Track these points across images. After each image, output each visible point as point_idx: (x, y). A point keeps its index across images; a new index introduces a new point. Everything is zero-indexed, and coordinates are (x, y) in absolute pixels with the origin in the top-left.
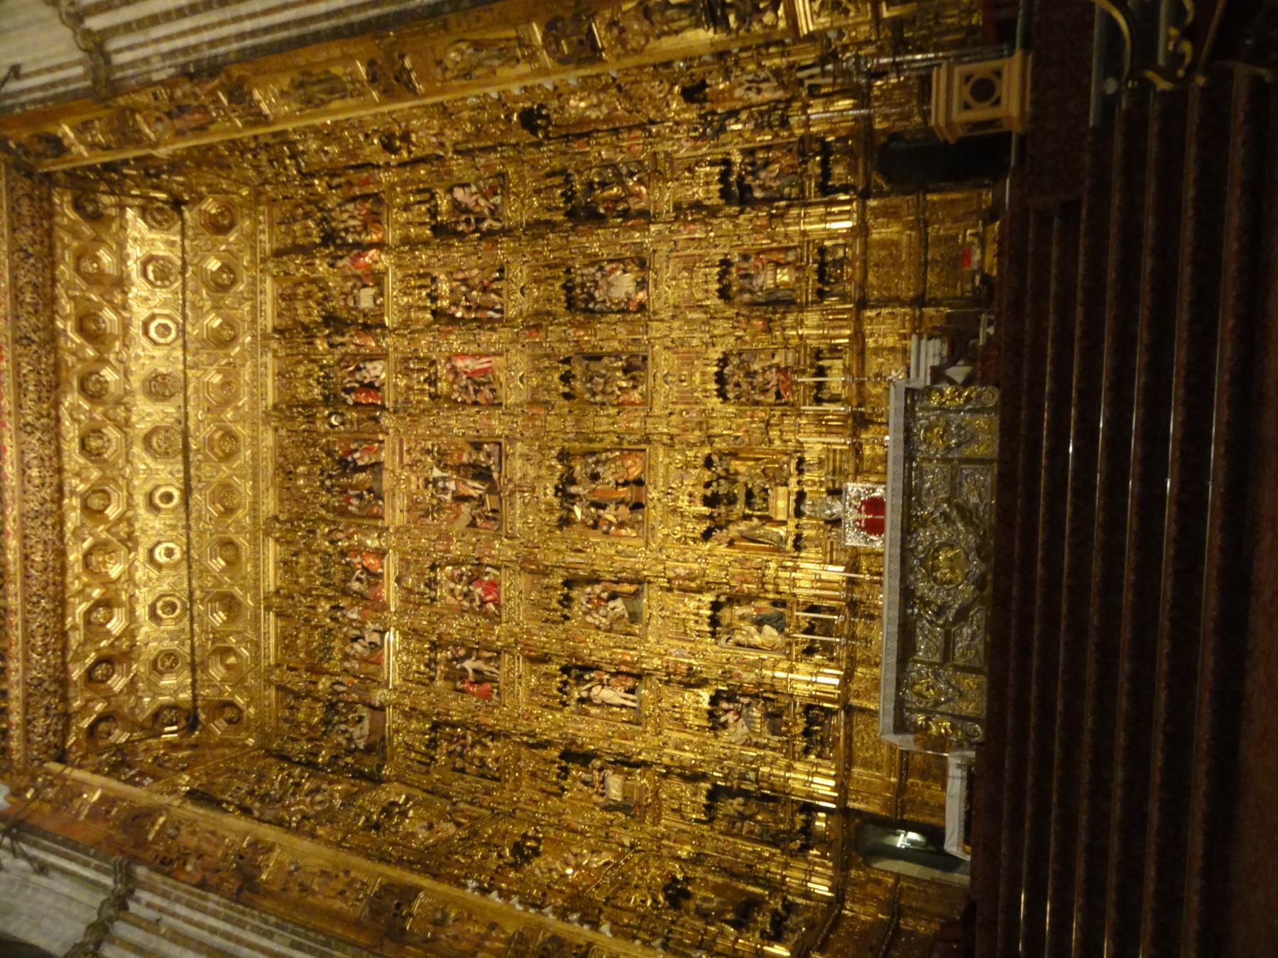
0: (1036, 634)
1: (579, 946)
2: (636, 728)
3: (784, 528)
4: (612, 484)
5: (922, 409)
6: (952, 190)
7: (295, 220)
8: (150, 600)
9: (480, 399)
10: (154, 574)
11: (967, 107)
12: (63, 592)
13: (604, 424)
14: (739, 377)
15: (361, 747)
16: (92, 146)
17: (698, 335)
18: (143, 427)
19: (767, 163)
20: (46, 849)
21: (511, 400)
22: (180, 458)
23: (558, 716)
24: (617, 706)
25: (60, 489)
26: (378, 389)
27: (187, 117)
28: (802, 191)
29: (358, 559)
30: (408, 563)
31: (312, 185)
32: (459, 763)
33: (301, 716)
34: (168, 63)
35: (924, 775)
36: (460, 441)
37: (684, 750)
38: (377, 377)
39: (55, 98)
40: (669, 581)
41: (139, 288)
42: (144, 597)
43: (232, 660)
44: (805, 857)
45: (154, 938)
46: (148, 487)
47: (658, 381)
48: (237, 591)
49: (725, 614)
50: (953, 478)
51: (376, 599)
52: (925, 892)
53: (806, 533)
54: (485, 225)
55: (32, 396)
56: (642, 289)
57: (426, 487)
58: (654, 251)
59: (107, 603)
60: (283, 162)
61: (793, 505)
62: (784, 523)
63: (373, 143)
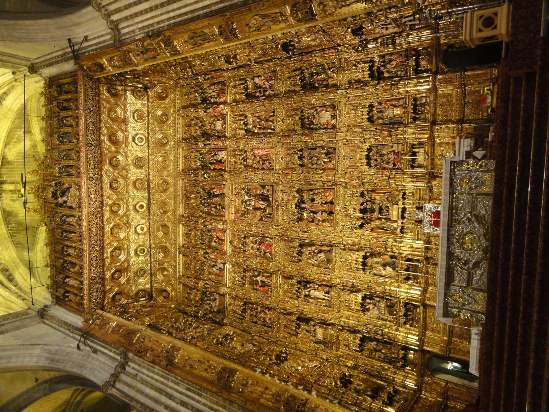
0: (510, 275)
1: (302, 400)
2: (329, 309)
3: (396, 224)
4: (320, 203)
5: (458, 170)
6: (478, 70)
7: (191, 94)
8: (135, 247)
9: (265, 167)
10: (136, 237)
11: (480, 30)
12: (103, 243)
13: (316, 177)
14: (377, 156)
15: (215, 310)
16: (114, 67)
18: (133, 178)
19: (390, 61)
20: (96, 343)
21: (278, 167)
22: (146, 191)
23: (296, 302)
25: (102, 203)
26: (223, 163)
27: (149, 53)
28: (406, 73)
29: (215, 233)
30: (235, 235)
31: (197, 79)
32: (255, 320)
33: (192, 297)
34: (142, 32)
35: (460, 337)
36: (256, 185)
37: (350, 320)
39: (100, 48)
40: (344, 246)
41: (131, 122)
42: (133, 246)
43: (166, 273)
44: (404, 370)
45: (135, 381)
46: (135, 203)
47: (340, 159)
48: (168, 245)
49: (369, 261)
50: (473, 202)
51: (222, 250)
52: (460, 390)
53: (406, 226)
54: (267, 93)
55: (92, 166)
56: (334, 119)
57: (242, 204)
58: (339, 102)
59: (119, 248)
61: (400, 214)
62: (396, 221)
63: (221, 61)
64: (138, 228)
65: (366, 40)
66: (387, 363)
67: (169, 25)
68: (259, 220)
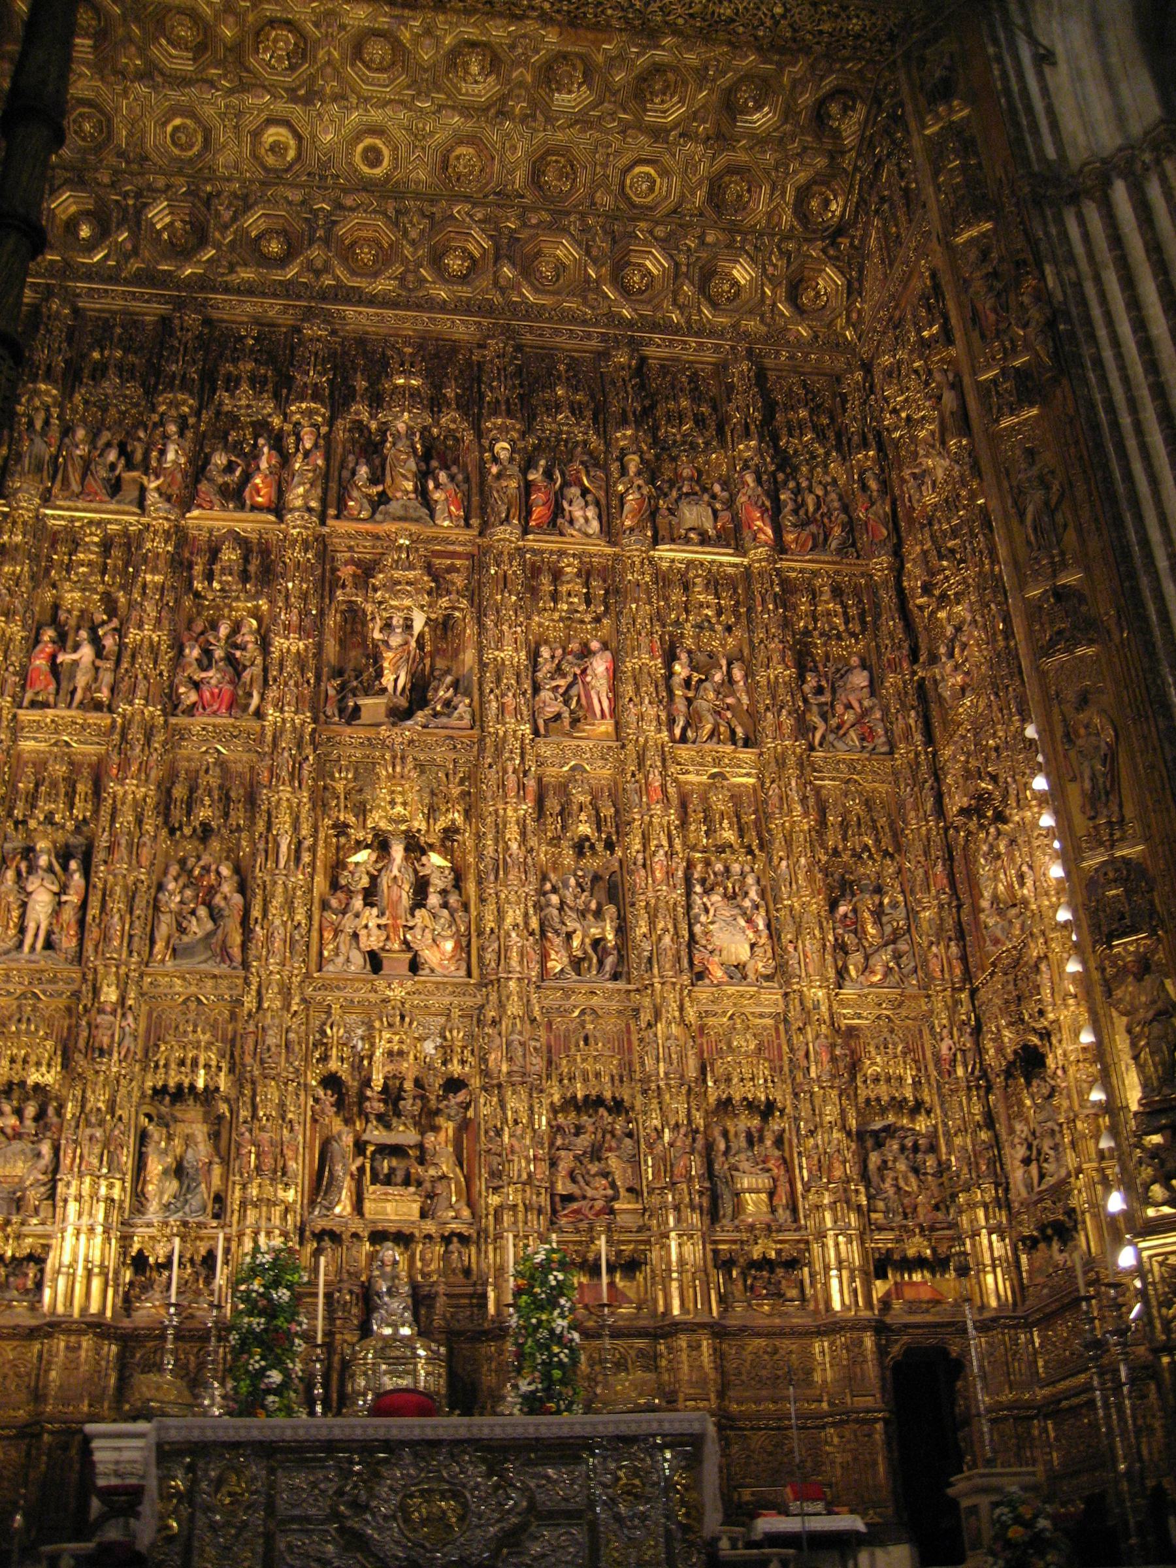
7: (812, 412)
9: (545, 695)
10: (251, 122)
19: (916, 1170)
24: (23, 916)
28: (880, 1229)
31: (865, 445)
38: (571, 522)
39: (1012, 110)
43: (85, 232)
60: (902, 408)
64: (283, 131)
65: (989, 1089)
67: (1092, 406)
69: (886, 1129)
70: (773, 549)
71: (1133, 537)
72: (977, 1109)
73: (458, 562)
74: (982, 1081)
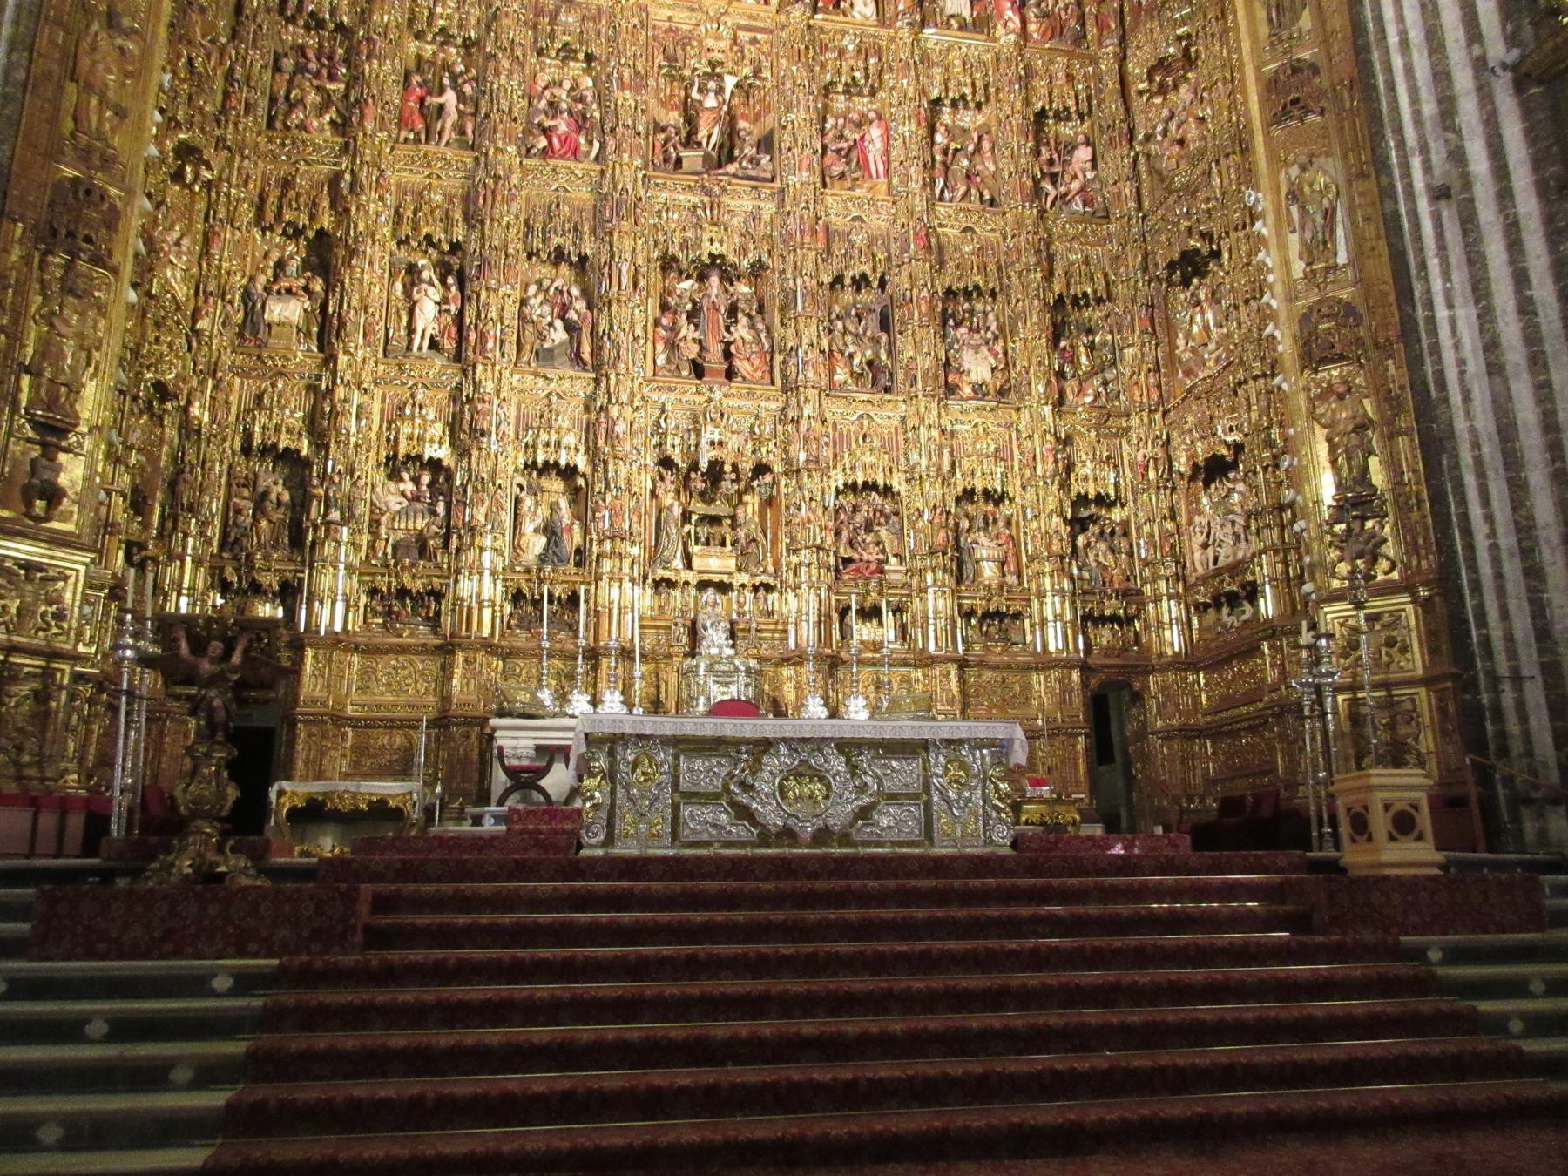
1: (110, 253)
3: (680, 566)
4: (728, 337)
11: (1387, 807)
17: (924, 462)
23: (387, 231)
30: (596, 19)
32: (288, 64)
35: (360, 750)
36: (770, 121)
44: (212, 586)
47: (861, 406)
49: (555, 485)
53: (677, 593)
54: (1047, 186)
56: (974, 391)
61: (716, 578)
63: (1168, 45)
65: (1174, 489)
66: (224, 535)
68: (656, 124)
69: (1091, 516)
70: (1019, 36)
71: (1369, 14)
72: (1164, 505)
73: (759, 36)
74: (1168, 482)
